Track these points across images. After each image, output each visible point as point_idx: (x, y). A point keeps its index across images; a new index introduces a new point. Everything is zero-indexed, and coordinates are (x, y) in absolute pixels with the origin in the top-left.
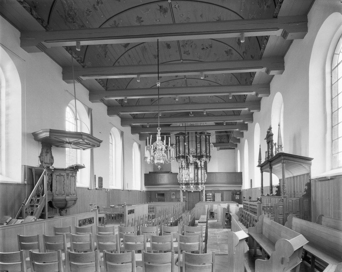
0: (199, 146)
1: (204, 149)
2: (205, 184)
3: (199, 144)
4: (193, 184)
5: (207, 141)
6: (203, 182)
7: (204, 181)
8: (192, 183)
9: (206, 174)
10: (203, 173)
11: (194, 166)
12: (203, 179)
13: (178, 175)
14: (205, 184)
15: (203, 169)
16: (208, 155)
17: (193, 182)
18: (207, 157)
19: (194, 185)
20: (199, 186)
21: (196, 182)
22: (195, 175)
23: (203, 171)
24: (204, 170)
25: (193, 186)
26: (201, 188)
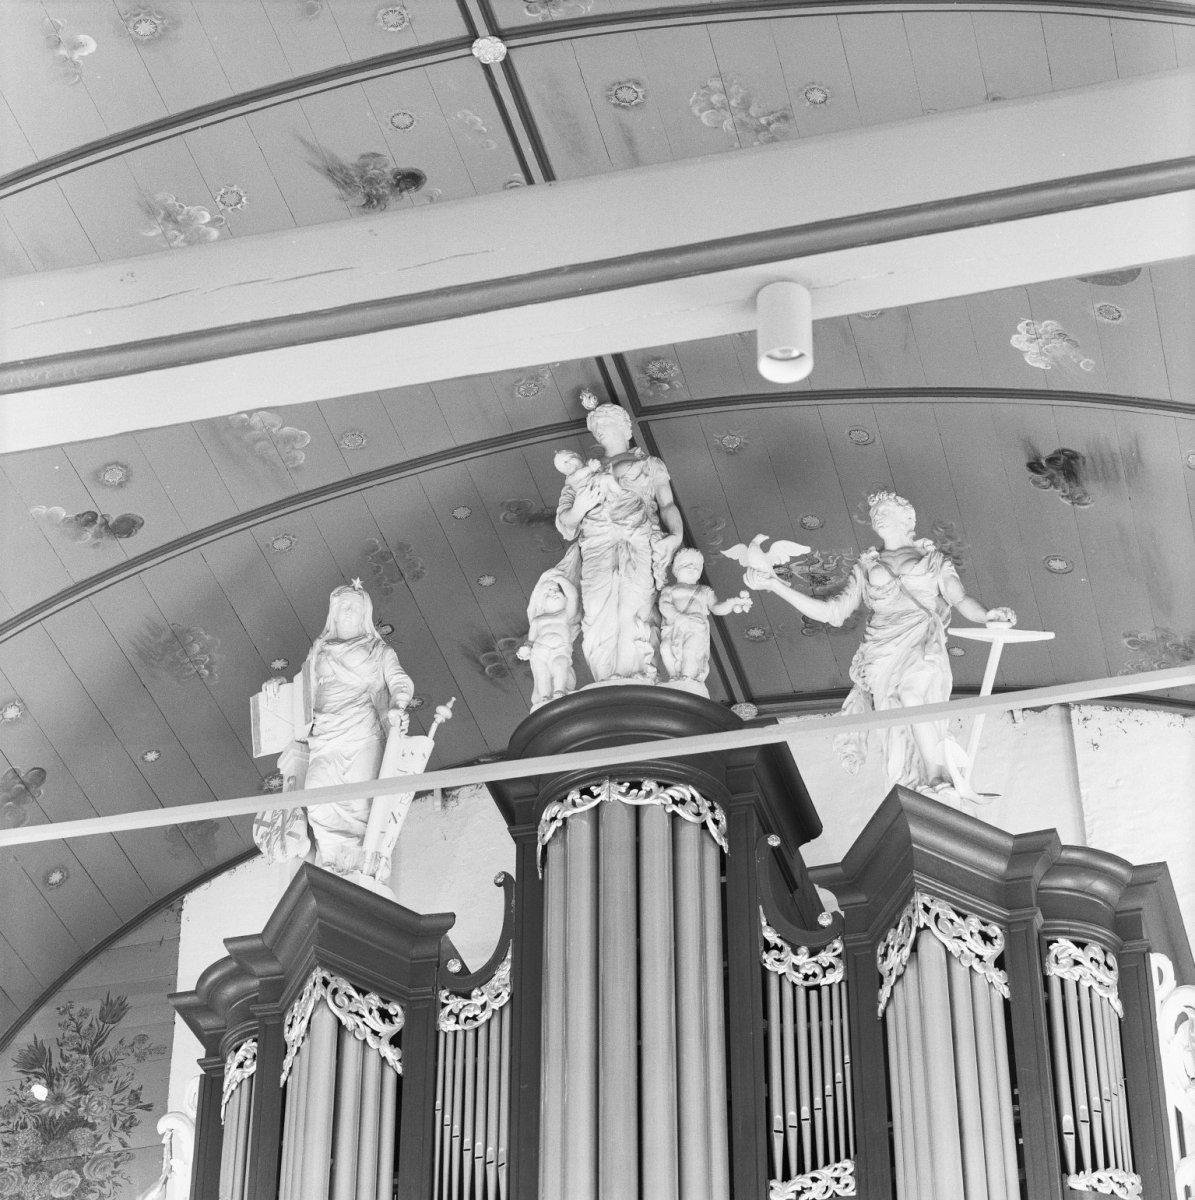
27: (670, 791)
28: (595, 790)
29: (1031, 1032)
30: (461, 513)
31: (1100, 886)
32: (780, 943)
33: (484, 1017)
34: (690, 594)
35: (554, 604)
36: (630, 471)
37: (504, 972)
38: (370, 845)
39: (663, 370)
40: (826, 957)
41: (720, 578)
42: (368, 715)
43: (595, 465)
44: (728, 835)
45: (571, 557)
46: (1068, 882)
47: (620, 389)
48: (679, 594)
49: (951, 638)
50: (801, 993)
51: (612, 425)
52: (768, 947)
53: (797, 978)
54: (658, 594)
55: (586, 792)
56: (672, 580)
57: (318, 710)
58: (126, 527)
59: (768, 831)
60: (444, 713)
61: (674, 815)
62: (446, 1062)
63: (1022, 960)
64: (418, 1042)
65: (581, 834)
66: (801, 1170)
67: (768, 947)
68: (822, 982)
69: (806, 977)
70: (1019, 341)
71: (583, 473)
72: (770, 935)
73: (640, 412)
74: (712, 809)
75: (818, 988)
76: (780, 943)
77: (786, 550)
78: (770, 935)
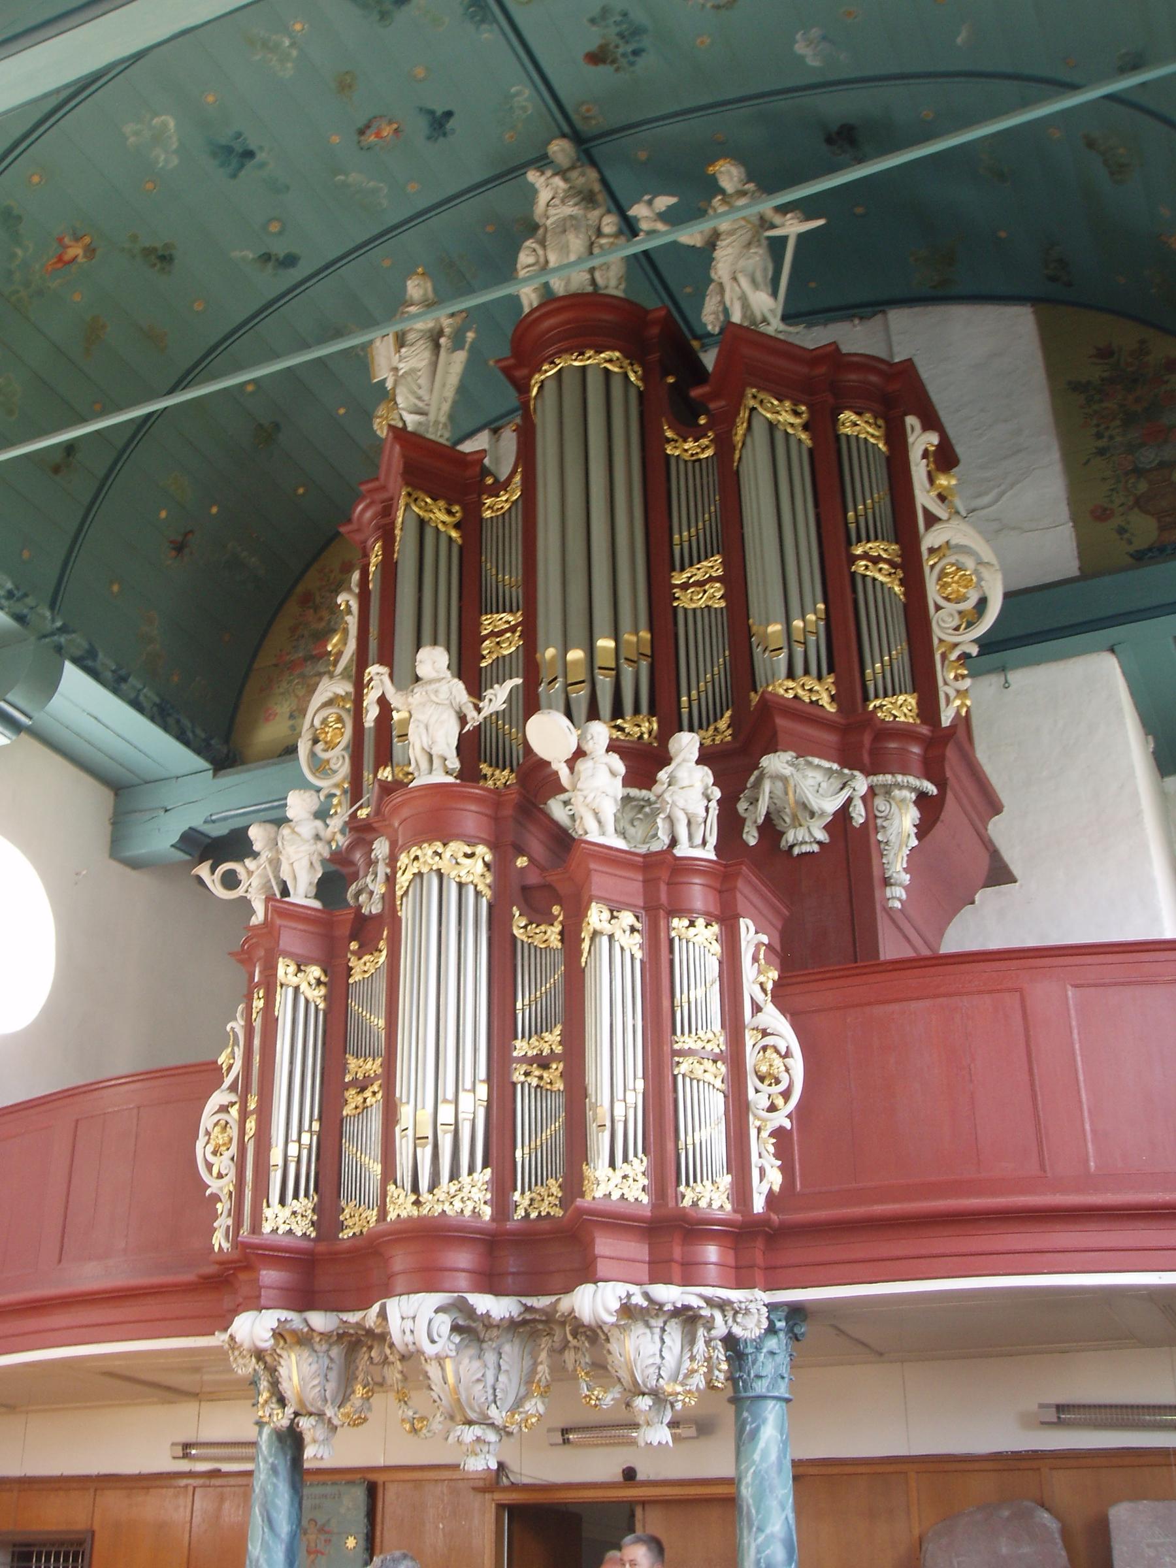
0: (700, 590)
1: (788, 625)
2: (762, 1244)
3: (713, 566)
4: (463, 1258)
5: (860, 506)
6: (710, 1195)
7: (741, 1192)
8: (433, 1234)
9: (774, 1018)
10: (699, 991)
11: (499, 868)
12: (704, 1128)
13: (219, 1097)
14: (762, 1244)
15: (698, 894)
16: (901, 708)
17: (469, 1197)
18: (858, 742)
19: (491, 1283)
20: (595, 1301)
21: (533, 1202)
22: (521, 1047)
23: (697, 942)
24: (727, 921)
25: (470, 1329)
26: (648, 1352)
27: (602, 355)
28: (557, 361)
29: (828, 463)
30: (490, 229)
31: (873, 378)
32: (675, 437)
33: (507, 506)
34: (611, 240)
35: (531, 260)
36: (574, 174)
37: (518, 478)
38: (432, 417)
39: (588, 110)
40: (705, 441)
41: (630, 228)
42: (429, 344)
43: (549, 173)
44: (643, 379)
45: (541, 231)
46: (853, 377)
47: (566, 129)
48: (603, 241)
49: (768, 238)
50: (690, 464)
51: (560, 150)
52: (668, 441)
53: (686, 456)
54: (592, 244)
55: (553, 362)
56: (599, 233)
57: (402, 346)
58: (290, 261)
59: (668, 374)
60: (470, 335)
61: (606, 370)
62: (487, 534)
63: (822, 424)
64: (471, 524)
65: (550, 387)
66: (691, 565)
67: (668, 441)
68: (702, 456)
69: (692, 455)
70: (800, 48)
71: (543, 179)
72: (669, 434)
73: (578, 139)
74: (631, 364)
75: (699, 460)
76: (675, 437)
77: (664, 202)
78: (669, 434)
